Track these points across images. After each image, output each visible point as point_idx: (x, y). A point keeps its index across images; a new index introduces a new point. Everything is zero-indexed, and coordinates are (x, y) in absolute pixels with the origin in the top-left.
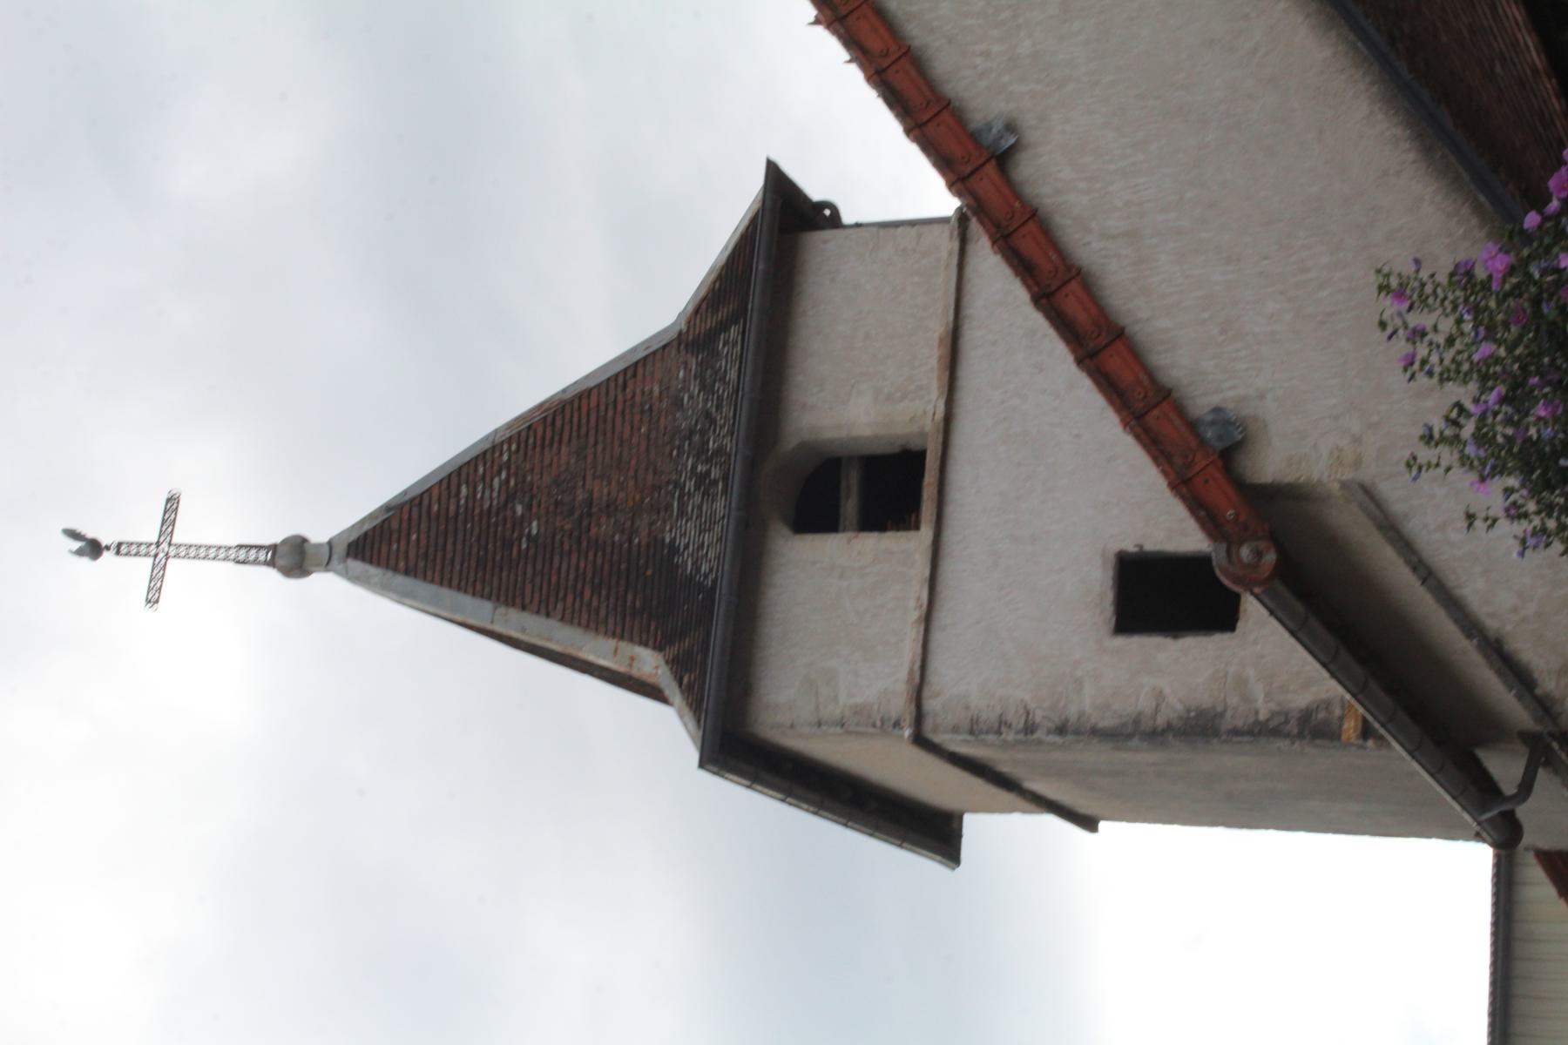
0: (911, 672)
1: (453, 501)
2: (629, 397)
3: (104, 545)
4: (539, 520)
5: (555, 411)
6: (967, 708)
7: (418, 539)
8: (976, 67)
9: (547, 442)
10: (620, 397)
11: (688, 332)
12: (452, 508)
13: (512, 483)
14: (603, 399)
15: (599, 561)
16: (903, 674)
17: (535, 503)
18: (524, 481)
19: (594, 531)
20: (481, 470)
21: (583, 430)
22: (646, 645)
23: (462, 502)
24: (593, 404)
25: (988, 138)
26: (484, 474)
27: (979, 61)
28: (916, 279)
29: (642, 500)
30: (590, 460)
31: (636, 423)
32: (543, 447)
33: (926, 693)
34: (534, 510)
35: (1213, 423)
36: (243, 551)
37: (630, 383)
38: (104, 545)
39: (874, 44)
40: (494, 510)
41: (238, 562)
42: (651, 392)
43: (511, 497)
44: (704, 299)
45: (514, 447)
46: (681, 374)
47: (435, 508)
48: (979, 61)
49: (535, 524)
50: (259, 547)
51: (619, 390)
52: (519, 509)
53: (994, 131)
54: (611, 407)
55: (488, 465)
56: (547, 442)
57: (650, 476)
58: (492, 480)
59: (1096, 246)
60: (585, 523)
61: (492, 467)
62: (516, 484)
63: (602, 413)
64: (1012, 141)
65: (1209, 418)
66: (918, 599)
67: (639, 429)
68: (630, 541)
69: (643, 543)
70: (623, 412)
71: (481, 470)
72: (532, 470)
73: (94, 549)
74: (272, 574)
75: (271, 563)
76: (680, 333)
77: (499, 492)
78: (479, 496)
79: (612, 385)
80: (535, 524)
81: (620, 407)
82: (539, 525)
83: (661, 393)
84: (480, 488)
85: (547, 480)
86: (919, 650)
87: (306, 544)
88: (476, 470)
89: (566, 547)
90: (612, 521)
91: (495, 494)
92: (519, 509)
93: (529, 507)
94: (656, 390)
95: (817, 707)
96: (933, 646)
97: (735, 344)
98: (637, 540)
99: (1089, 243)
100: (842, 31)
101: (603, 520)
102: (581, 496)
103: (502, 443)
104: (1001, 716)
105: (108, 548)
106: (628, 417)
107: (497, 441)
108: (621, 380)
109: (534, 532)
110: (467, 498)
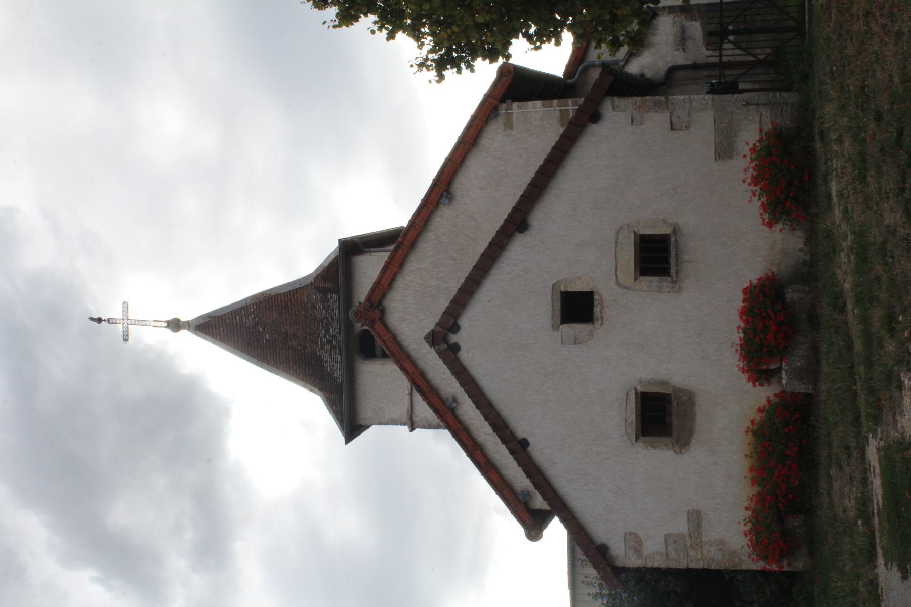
0: (408, 410)
1: (234, 320)
2: (296, 299)
3: (103, 319)
4: (268, 334)
5: (268, 299)
6: (427, 420)
7: (223, 330)
8: (441, 377)
9: (267, 308)
10: (292, 299)
11: (314, 283)
12: (235, 322)
13: (256, 319)
14: (286, 298)
16: (405, 409)
17: (266, 328)
19: (290, 343)
22: (315, 387)
23: (238, 321)
24: (283, 299)
26: (245, 314)
27: (441, 375)
28: (399, 309)
29: (307, 337)
30: (284, 318)
33: (414, 415)
34: (266, 330)
35: (521, 494)
36: (156, 322)
38: (103, 319)
41: (155, 326)
42: (304, 300)
44: (319, 275)
45: (255, 307)
46: (314, 297)
48: (441, 375)
49: (267, 335)
50: (162, 321)
51: (292, 297)
52: (261, 329)
53: (449, 401)
54: (289, 301)
55: (246, 311)
56: (267, 308)
58: (248, 317)
60: (286, 339)
62: (258, 320)
64: (455, 404)
65: (520, 493)
66: (408, 387)
67: (301, 312)
68: (304, 350)
69: (309, 352)
70: (295, 305)
72: (263, 317)
73: (99, 320)
74: (168, 330)
76: (312, 282)
77: (252, 321)
78: (244, 321)
79: (289, 294)
80: (267, 335)
81: (293, 303)
82: (269, 336)
83: (307, 301)
84: (244, 318)
86: (410, 404)
87: (180, 322)
88: (241, 311)
91: (250, 322)
92: (261, 329)
93: (264, 329)
94: (306, 300)
95: (379, 420)
98: (307, 350)
99: (480, 436)
100: (399, 365)
101: (293, 340)
102: (283, 330)
104: (438, 424)
105: (104, 320)
106: (296, 306)
107: (248, 304)
108: (292, 293)
109: (268, 338)
110: (240, 321)
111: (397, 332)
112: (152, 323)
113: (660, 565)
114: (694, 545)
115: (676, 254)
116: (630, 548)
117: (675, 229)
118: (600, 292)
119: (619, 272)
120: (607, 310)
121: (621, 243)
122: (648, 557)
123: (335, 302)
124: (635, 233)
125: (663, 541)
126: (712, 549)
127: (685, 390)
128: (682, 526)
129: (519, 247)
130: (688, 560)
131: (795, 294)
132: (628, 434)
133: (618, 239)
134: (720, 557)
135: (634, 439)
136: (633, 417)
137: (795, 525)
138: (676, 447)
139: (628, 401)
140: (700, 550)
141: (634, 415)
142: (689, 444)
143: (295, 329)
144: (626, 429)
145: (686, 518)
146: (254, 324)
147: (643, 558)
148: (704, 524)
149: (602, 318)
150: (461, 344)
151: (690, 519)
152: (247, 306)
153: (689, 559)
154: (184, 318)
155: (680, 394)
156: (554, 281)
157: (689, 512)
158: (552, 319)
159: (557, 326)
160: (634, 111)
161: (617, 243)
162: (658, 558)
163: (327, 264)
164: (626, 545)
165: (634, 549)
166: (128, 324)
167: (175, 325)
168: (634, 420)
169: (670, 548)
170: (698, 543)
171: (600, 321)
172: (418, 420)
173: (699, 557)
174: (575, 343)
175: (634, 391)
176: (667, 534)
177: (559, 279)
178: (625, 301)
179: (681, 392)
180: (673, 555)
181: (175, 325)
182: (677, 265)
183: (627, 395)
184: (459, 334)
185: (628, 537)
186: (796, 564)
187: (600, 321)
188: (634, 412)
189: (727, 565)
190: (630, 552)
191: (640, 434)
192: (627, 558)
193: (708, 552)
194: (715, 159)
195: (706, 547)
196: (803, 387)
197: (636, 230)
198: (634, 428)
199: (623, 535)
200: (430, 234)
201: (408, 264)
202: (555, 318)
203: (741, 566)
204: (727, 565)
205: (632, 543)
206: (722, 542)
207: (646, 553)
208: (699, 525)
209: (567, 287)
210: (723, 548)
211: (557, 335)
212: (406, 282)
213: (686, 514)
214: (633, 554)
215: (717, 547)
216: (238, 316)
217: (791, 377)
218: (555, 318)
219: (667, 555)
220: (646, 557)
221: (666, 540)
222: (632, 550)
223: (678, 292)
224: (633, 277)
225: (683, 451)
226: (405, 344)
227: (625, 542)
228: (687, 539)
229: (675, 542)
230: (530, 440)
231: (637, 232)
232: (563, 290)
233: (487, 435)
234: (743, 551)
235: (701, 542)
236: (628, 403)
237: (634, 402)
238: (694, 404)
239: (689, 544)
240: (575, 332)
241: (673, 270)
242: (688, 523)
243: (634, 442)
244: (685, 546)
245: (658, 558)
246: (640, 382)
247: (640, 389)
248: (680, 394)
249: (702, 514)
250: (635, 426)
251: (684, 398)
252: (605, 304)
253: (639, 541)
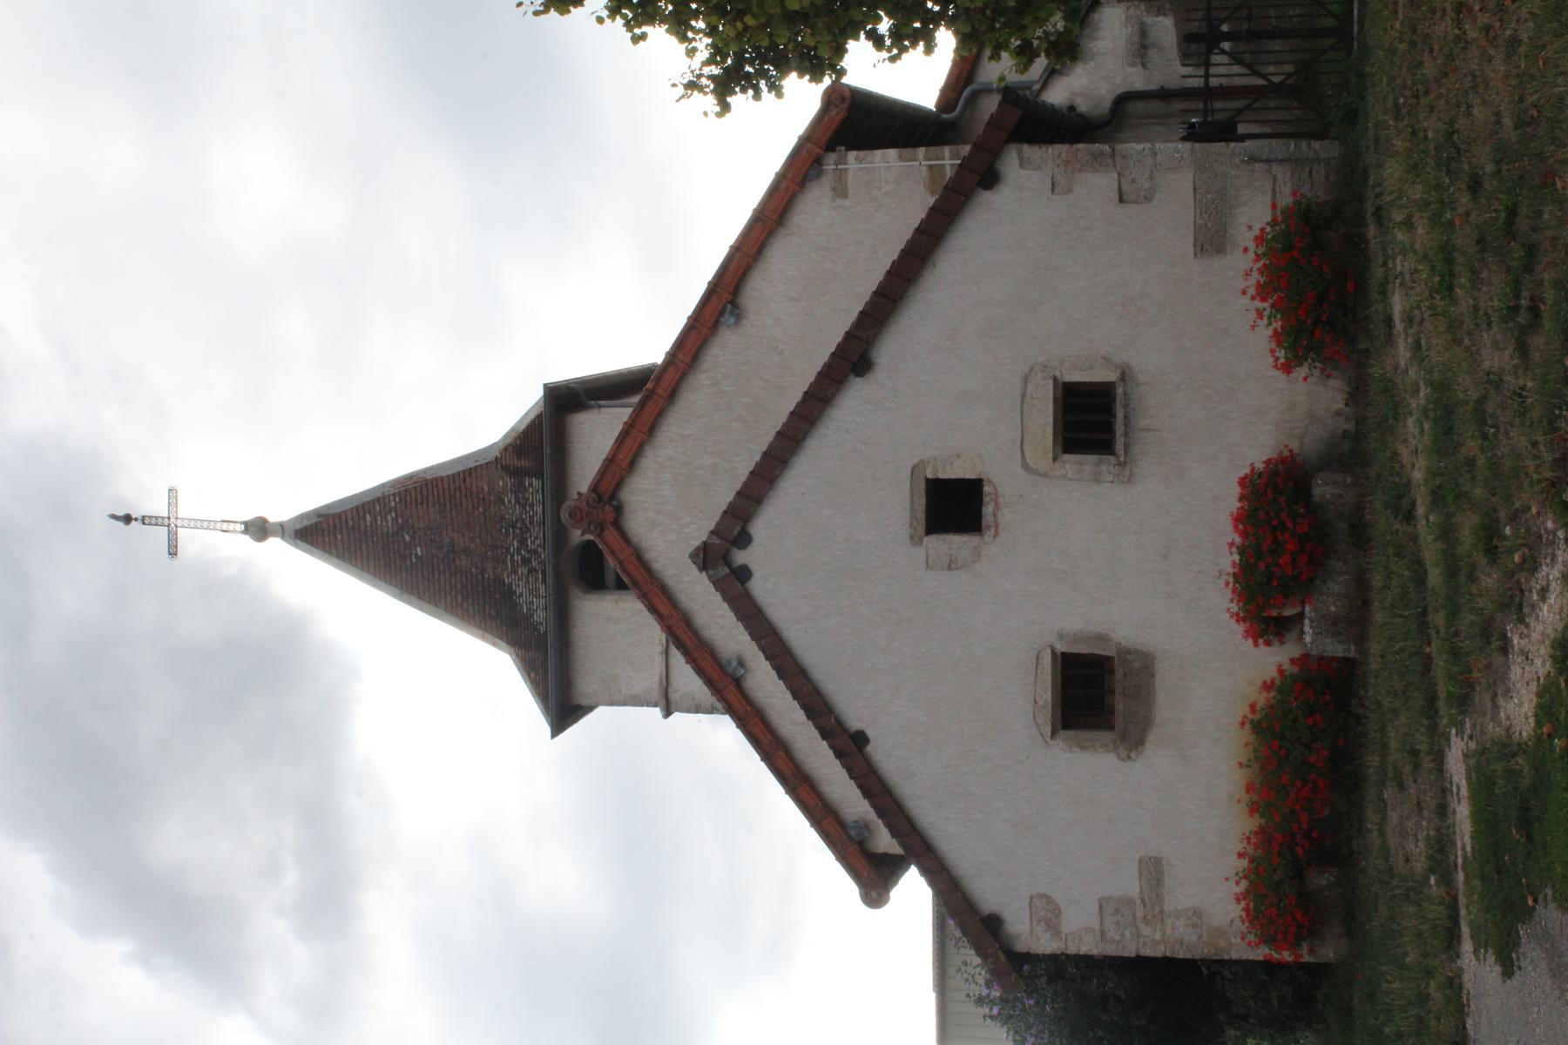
0: (661, 679)
1: (361, 521)
2: (468, 487)
3: (134, 517)
4: (421, 547)
5: (421, 485)
6: (694, 699)
7: (342, 538)
9: (419, 502)
10: (463, 486)
11: (501, 458)
12: (362, 526)
13: (400, 521)
14: (452, 485)
15: (464, 581)
16: (656, 680)
17: (416, 536)
18: (407, 522)
19: (458, 562)
20: (378, 508)
21: (442, 500)
22: (502, 639)
23: (368, 524)
25: (730, 669)
27: (719, 620)
30: (449, 519)
31: (476, 505)
32: (416, 506)
33: (670, 690)
34: (417, 539)
37: (468, 479)
38: (134, 517)
39: (664, 610)
40: (391, 534)
41: (223, 531)
42: (483, 488)
43: (401, 529)
44: (510, 445)
45: (397, 499)
46: (501, 483)
47: (351, 523)
48: (719, 620)
49: (419, 549)
50: (237, 522)
51: (462, 482)
52: (407, 538)
54: (457, 490)
55: (382, 506)
56: (419, 502)
57: (489, 540)
58: (386, 515)
59: (789, 727)
60: (451, 556)
61: (385, 508)
62: (403, 521)
63: (452, 493)
64: (743, 672)
65: (852, 824)
66: (660, 640)
67: (478, 509)
69: (492, 577)
70: (466, 496)
72: (412, 517)
73: (127, 519)
74: (247, 538)
76: (496, 458)
78: (379, 523)
79: (456, 477)
80: (419, 549)
81: (464, 492)
82: (422, 551)
84: (379, 518)
85: (422, 525)
86: (664, 669)
87: (266, 525)
88: (374, 507)
89: (441, 568)
90: (469, 560)
91: (390, 525)
92: (407, 538)
93: (413, 538)
94: (486, 487)
95: (610, 696)
96: (671, 665)
100: (646, 603)
101: (463, 557)
102: (446, 540)
103: (389, 496)
105: (136, 519)
106: (469, 499)
107: (386, 494)
108: (462, 476)
109: (419, 553)
110: (371, 522)
111: (644, 545)
112: (219, 526)
113: (1090, 950)
114: (1149, 917)
116: (1040, 920)
117: (1123, 373)
118: (994, 480)
119: (1026, 447)
121: (1032, 397)
122: (1069, 937)
123: (538, 492)
124: (1055, 379)
126: (1180, 924)
127: (1136, 652)
128: (1128, 885)
129: (855, 398)
130: (1138, 942)
131: (1327, 488)
132: (1038, 725)
133: (1025, 389)
134: (1195, 938)
135: (1049, 734)
136: (1048, 696)
138: (1121, 748)
141: (1050, 692)
143: (466, 538)
146: (395, 528)
147: (1061, 940)
148: (1167, 880)
150: (753, 567)
151: (1144, 873)
153: (1141, 941)
155: (1129, 657)
156: (915, 461)
157: (1140, 860)
158: (911, 526)
161: (1023, 396)
163: (523, 427)
165: (1046, 922)
167: (259, 529)
168: (1050, 700)
169: (1109, 921)
171: (993, 531)
173: (1158, 936)
174: (950, 568)
175: (1050, 652)
176: (1103, 898)
177: (924, 457)
180: (1112, 933)
181: (259, 529)
182: (1126, 435)
183: (1038, 657)
187: (993, 531)
188: (1050, 687)
189: (1206, 951)
192: (1034, 937)
193: (1173, 929)
194: (1195, 254)
195: (1169, 921)
196: (1340, 647)
197: (1058, 374)
198: (1050, 716)
200: (702, 376)
201: (664, 428)
203: (1229, 954)
204: (1206, 951)
205: (1043, 913)
206: (1197, 912)
208: (1159, 882)
210: (1199, 922)
211: (919, 553)
212: (661, 459)
213: (1136, 865)
214: (1046, 932)
215: (1189, 922)
216: (368, 516)
217: (1320, 630)
218: (915, 523)
219: (1103, 934)
220: (1066, 936)
221: (1101, 908)
222: (1043, 924)
224: (1051, 455)
225: (1133, 755)
226: (656, 566)
228: (1138, 905)
229: (1117, 911)
230: (870, 734)
232: (929, 476)
233: (796, 724)
234: (1234, 928)
235: (1162, 912)
236: (1039, 671)
237: (1050, 670)
238: (1153, 676)
239: (1140, 914)
240: (950, 549)
241: (1119, 444)
242: (1140, 880)
243: (1048, 739)
244: (1134, 917)
247: (1061, 648)
248: (1129, 657)
249: (1164, 863)
250: (1050, 712)
252: (1001, 500)
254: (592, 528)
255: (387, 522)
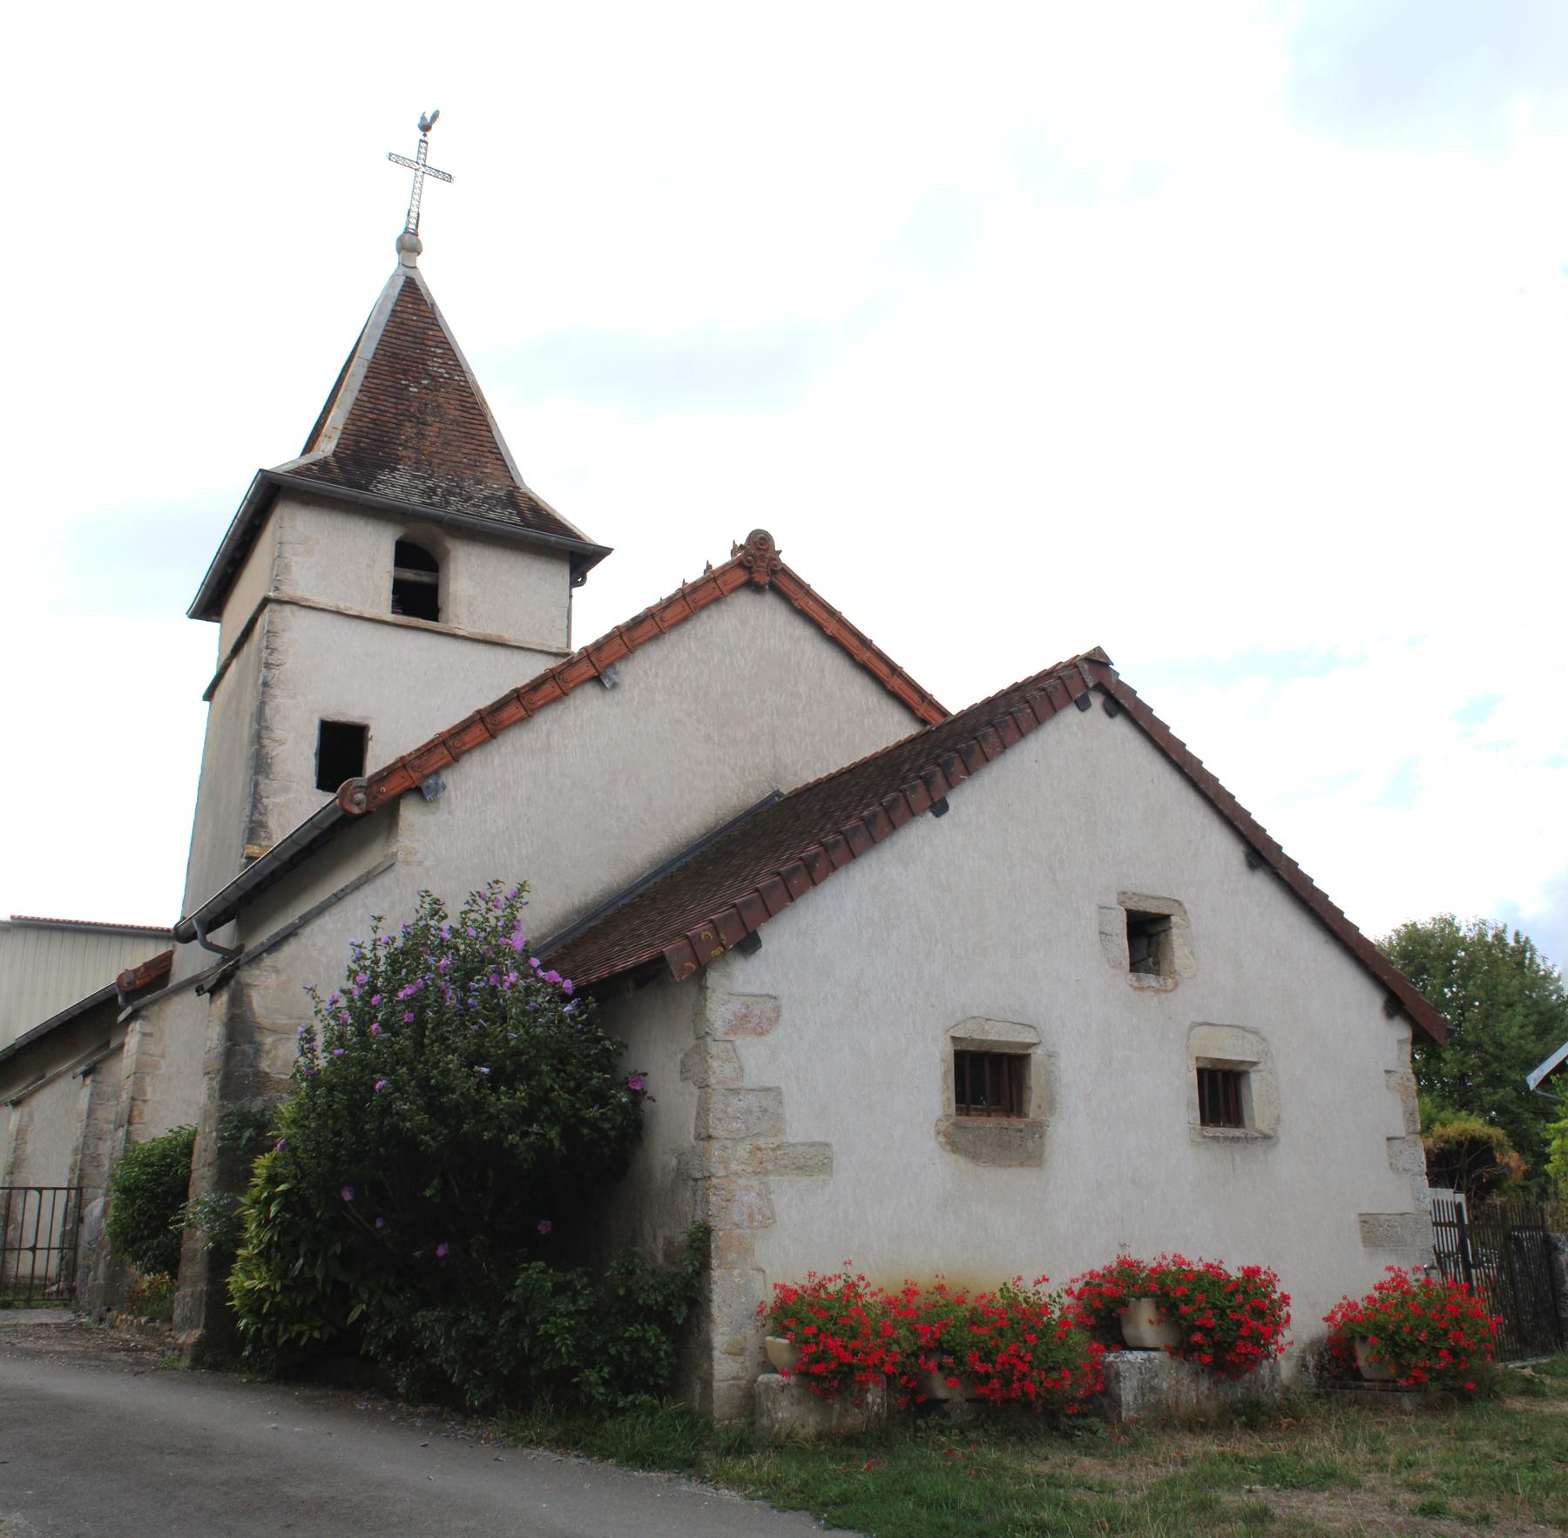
0: (308, 600)
1: (433, 343)
6: (283, 631)
7: (413, 320)
12: (430, 343)
14: (485, 439)
15: (390, 425)
16: (307, 595)
18: (441, 387)
19: (408, 424)
20: (451, 363)
21: (468, 425)
24: (483, 433)
25: (610, 672)
29: (424, 455)
30: (450, 427)
31: (469, 457)
32: (460, 400)
34: (424, 391)
35: (437, 784)
37: (493, 456)
39: (668, 614)
40: (426, 367)
43: (433, 378)
44: (537, 505)
45: (462, 383)
47: (431, 333)
48: (653, 670)
49: (416, 390)
50: (417, 227)
52: (425, 382)
57: (437, 461)
59: (544, 727)
60: (413, 419)
63: (477, 437)
64: (607, 686)
65: (440, 782)
68: (400, 445)
70: (476, 450)
71: (451, 363)
73: (425, 128)
75: (407, 231)
79: (493, 445)
80: (416, 390)
81: (479, 448)
84: (440, 361)
85: (441, 400)
89: (400, 407)
92: (425, 382)
93: (426, 388)
94: (488, 471)
95: (291, 543)
96: (322, 615)
97: (510, 519)
101: (415, 431)
102: (430, 419)
105: (425, 135)
106: (473, 452)
108: (495, 450)
110: (434, 352)
111: (724, 607)
112: (414, 209)
113: (714, 1073)
114: (760, 1155)
115: (1239, 1138)
116: (748, 1007)
117: (1266, 1137)
118: (1178, 989)
119: (1206, 1028)
120: (1155, 999)
121: (1244, 1038)
122: (729, 1045)
123: (510, 519)
124: (1255, 1064)
125: (768, 1085)
126: (751, 1198)
127: (1043, 1145)
128: (799, 1128)
129: (1230, 851)
130: (727, 1139)
131: (1268, 1370)
132: (965, 1021)
133: (1248, 1031)
134: (736, 1218)
135: (956, 1035)
136: (993, 1037)
137: (869, 1395)
138: (947, 1124)
139: (1020, 1027)
140: (750, 1169)
141: (996, 1038)
142: (954, 1152)
143: (435, 439)
144: (973, 1018)
145: (817, 1138)
146: (433, 373)
147: (726, 1034)
148: (804, 1181)
149: (1141, 989)
150: (1089, 713)
151: (812, 1149)
152: (463, 371)
153: (729, 1144)
154: (421, 261)
155: (1037, 1136)
156: (1186, 905)
157: (828, 1145)
158: (1134, 894)
159: (1123, 902)
160: (1399, 1075)
161: (1243, 1029)
162: (728, 1070)
163: (558, 518)
164: (755, 999)
165: (746, 1016)
166: (416, 170)
167: (409, 246)
168: (989, 1038)
169: (751, 1099)
170: (765, 1164)
171: (1136, 984)
172: (285, 614)
173: (734, 1167)
174: (1101, 933)
175: (1036, 1041)
176: (780, 1094)
177: (1189, 915)
178: (1171, 1036)
179: (1040, 1137)
180: (736, 1104)
181: (409, 246)
182: (1226, 1139)
183: (1030, 1026)
184: (1103, 714)
185: (771, 1003)
186: (784, 1404)
187: (1136, 984)
188: (1002, 1039)
189: (721, 1233)
190: (739, 1006)
191: (959, 1048)
192: (725, 997)
193: (746, 1188)
194: (1361, 1215)
195: (755, 1182)
196: (1130, 1398)
197: (1260, 1067)
198: (975, 1036)
199: (774, 994)
200: (875, 700)
201: (830, 653)
202: (1136, 899)
203: (719, 1266)
204: (721, 1233)
205: (757, 1012)
206: (768, 1222)
207: (739, 1041)
208: (801, 1169)
209: (1178, 928)
210: (756, 1224)
211: (1112, 900)
212: (802, 642)
213: (822, 1139)
214: (734, 1013)
215: (756, 1210)
216: (441, 351)
217: (1143, 1371)
218: (1136, 899)
219: (735, 1091)
220: (731, 1041)
221: (769, 1090)
222: (744, 1011)
223: (1192, 1141)
224: (1202, 1055)
225: (941, 1139)
226: (704, 615)
227: (761, 996)
228: (771, 1140)
229: (765, 1111)
230: (945, 818)
231: (1255, 1068)
232: (1173, 918)
233: (548, 736)
234: (751, 1272)
235: (767, 1173)
236: (1017, 1026)
237: (1018, 1040)
238: (1022, 1165)
239: (761, 1142)
240: (1117, 935)
241: (1212, 1131)
242: (804, 1144)
243: (951, 1033)
244: (757, 1135)
245: (728, 1070)
246: (1050, 1056)
247: (1037, 1055)
248: (1037, 1136)
249: (822, 1177)
250: (978, 1037)
251: (1030, 1144)
252: (1163, 996)
253: (762, 1028)
254: (750, 558)
255: (439, 368)
